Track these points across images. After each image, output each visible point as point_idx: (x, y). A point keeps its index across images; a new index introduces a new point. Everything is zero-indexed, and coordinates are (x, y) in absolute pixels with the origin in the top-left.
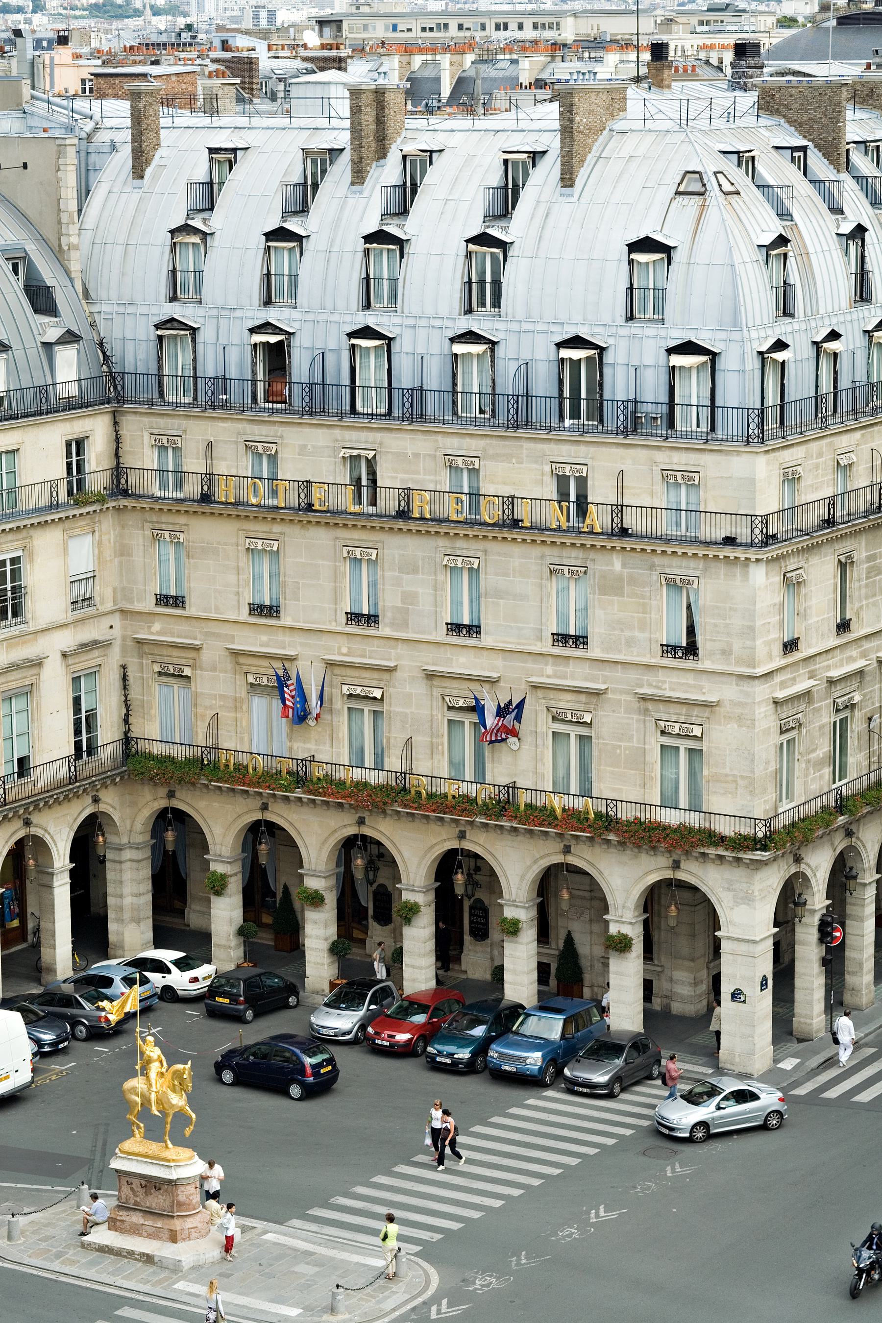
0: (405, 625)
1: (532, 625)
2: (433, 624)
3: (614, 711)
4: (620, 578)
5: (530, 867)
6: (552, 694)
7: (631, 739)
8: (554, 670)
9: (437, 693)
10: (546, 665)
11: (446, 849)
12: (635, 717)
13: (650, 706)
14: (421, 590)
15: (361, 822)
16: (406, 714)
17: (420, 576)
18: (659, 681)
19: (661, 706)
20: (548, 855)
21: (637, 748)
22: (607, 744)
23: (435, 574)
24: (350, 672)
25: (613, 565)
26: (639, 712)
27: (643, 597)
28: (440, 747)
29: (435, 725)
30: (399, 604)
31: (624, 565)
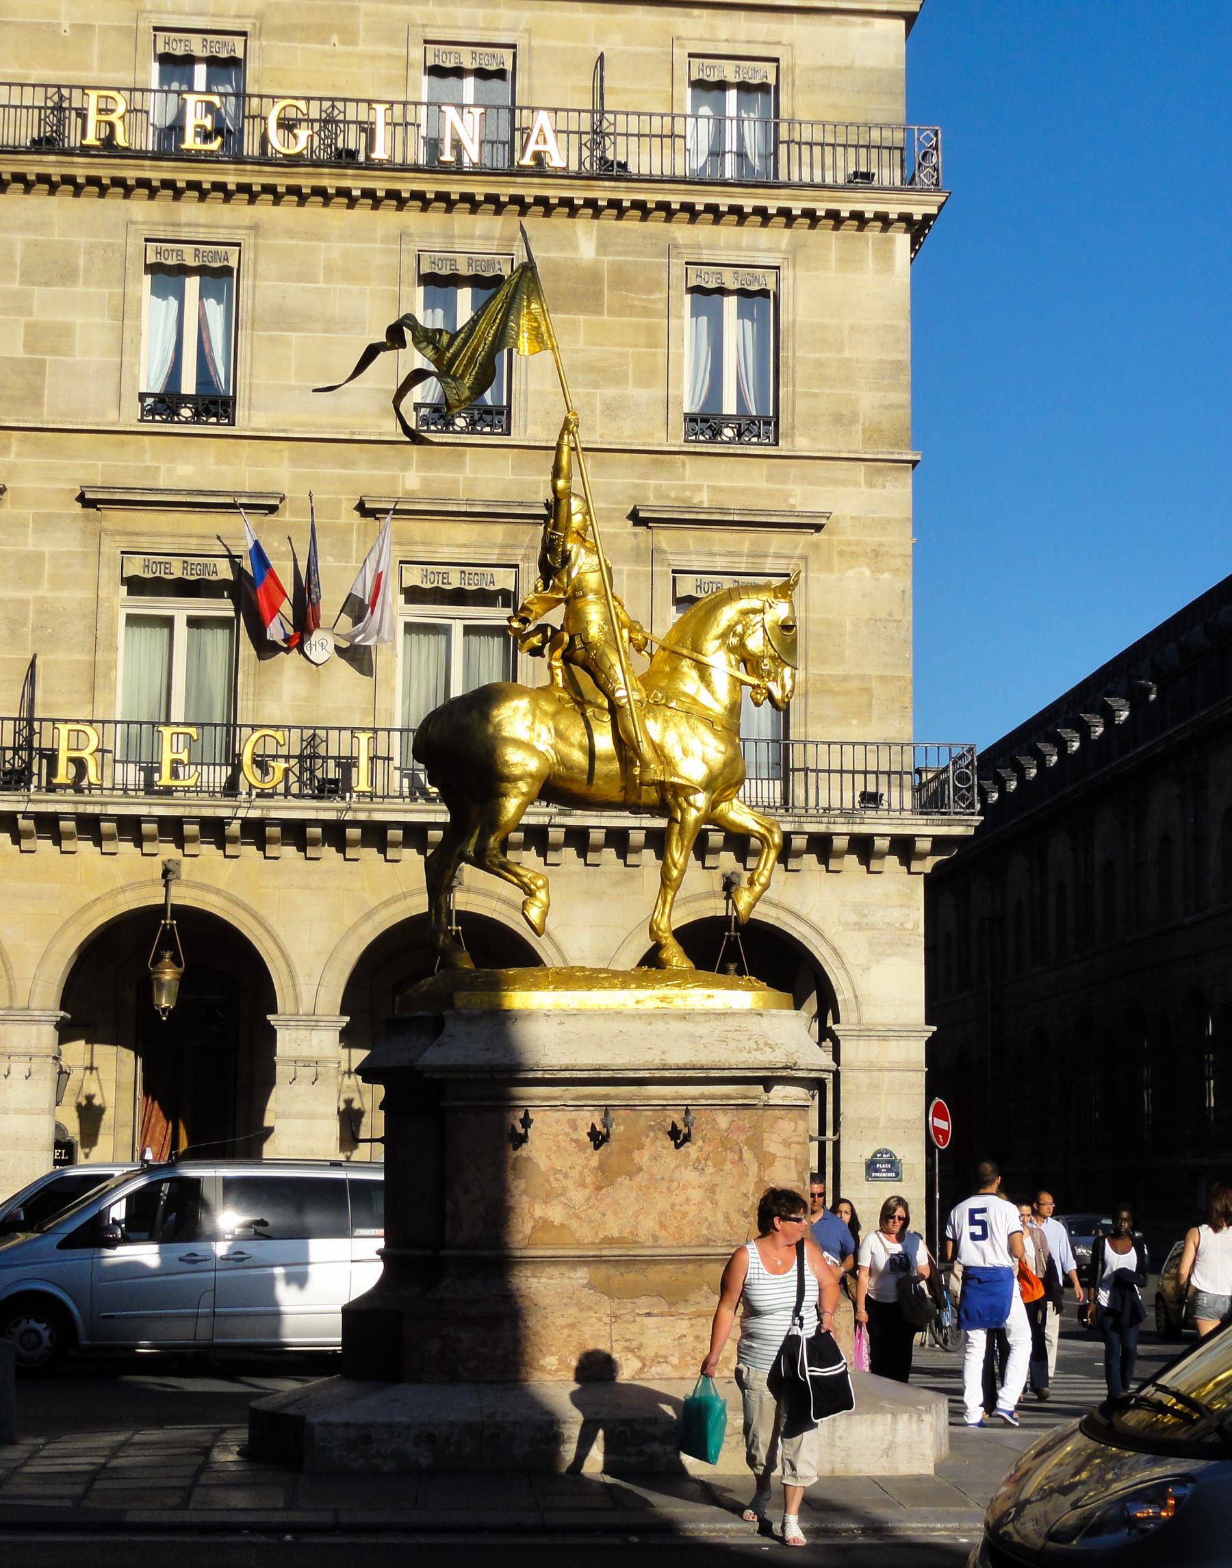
0: (34, 396)
2: (111, 395)
4: (593, 276)
5: (355, 926)
6: (417, 528)
8: (424, 479)
9: (112, 548)
10: (405, 468)
13: (664, 538)
14: (78, 320)
16: (24, 603)
17: (80, 289)
18: (684, 488)
25: (575, 248)
26: (636, 555)
27: (646, 312)
30: (20, 353)
31: (602, 247)
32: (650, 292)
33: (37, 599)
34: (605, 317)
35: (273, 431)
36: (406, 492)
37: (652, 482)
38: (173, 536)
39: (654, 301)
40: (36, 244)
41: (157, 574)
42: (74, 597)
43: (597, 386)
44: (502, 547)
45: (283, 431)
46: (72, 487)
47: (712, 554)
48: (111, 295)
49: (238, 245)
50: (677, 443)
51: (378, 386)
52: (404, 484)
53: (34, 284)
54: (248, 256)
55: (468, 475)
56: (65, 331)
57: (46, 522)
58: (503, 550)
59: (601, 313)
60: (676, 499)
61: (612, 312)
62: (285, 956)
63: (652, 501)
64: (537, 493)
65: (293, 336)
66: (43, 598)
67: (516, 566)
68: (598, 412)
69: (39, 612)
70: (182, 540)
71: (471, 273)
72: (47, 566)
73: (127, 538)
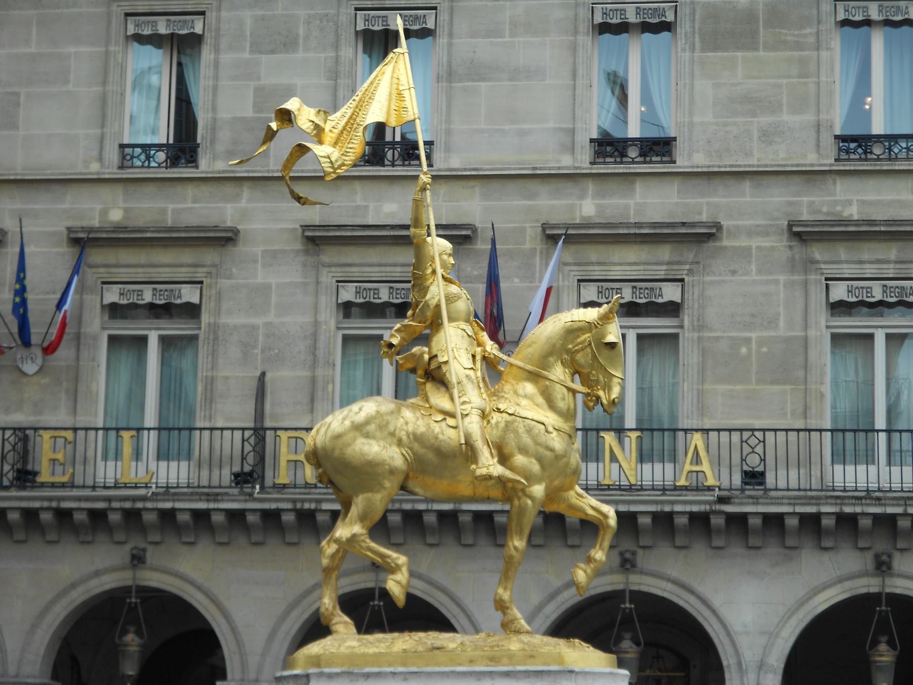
1: (551, 125)
3: (734, 272)
7: (773, 322)
8: (598, 206)
9: (328, 278)
10: (582, 197)
12: (782, 278)
13: (817, 252)
15: (138, 559)
16: (254, 328)
17: (300, 55)
18: (836, 203)
19: (842, 251)
21: (788, 340)
22: (717, 339)
23: (336, 47)
24: (126, 256)
26: (792, 266)
28: (330, 387)
29: (321, 344)
30: (249, 113)
32: (802, 27)
33: (268, 325)
34: (762, 53)
35: (465, 170)
36: (583, 218)
37: (805, 199)
38: (380, 265)
39: (805, 36)
40: (263, 18)
41: (367, 299)
42: (297, 321)
43: (754, 114)
44: (669, 263)
45: (474, 169)
46: (291, 226)
47: (861, 262)
48: (326, 59)
49: (435, 8)
50: (828, 160)
51: (557, 126)
52: (581, 211)
53: (261, 52)
54: (444, 17)
55: (638, 200)
57: (273, 257)
58: (670, 267)
59: (757, 49)
60: (828, 214)
61: (767, 48)
63: (805, 217)
64: (700, 213)
65: (483, 84)
66: (271, 323)
67: (682, 280)
68: (755, 138)
69: (267, 336)
70: (388, 269)
71: (638, 20)
72: (273, 296)
73: (339, 269)
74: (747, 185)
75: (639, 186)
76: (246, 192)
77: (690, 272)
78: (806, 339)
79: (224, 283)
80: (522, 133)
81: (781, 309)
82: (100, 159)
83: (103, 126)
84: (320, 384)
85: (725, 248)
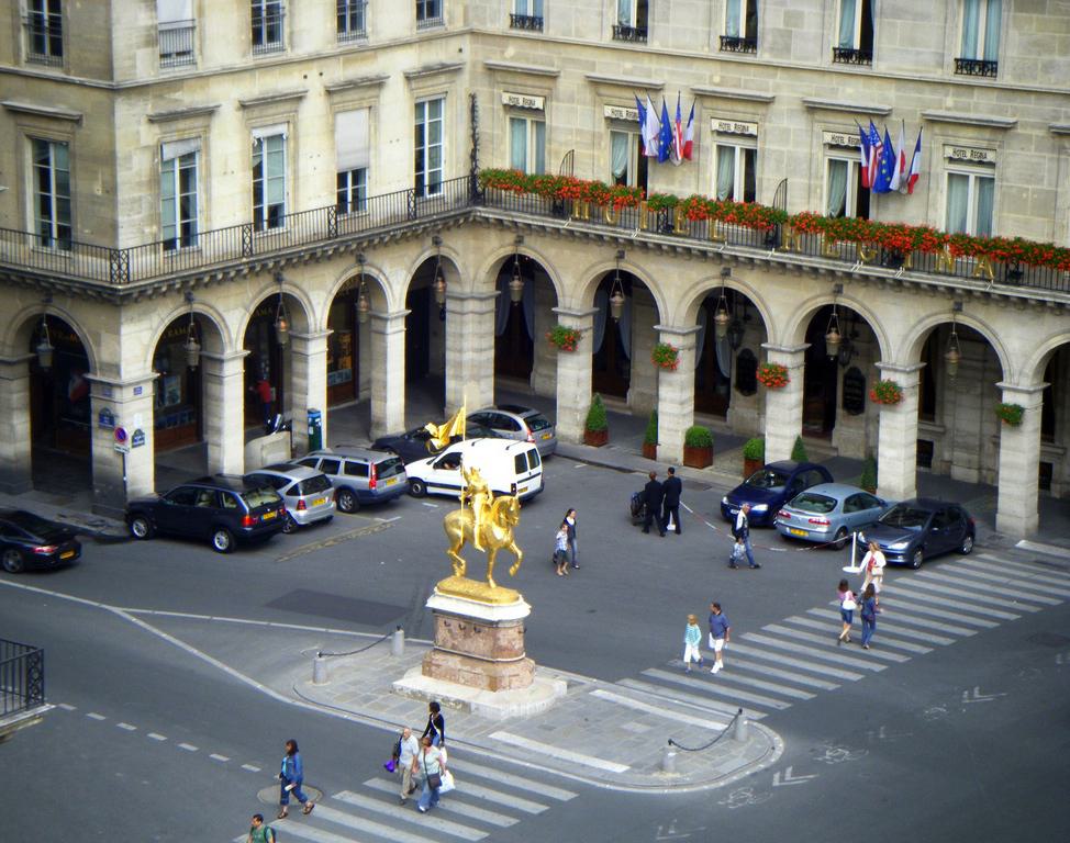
0: (787, 49)
1: (933, 50)
2: (818, 50)
3: (1022, 149)
6: (951, 130)
8: (955, 102)
10: (947, 95)
11: (820, 304)
12: (1048, 155)
16: (782, 152)
20: (936, 314)
21: (1048, 192)
28: (818, 191)
29: (814, 166)
30: (781, 26)
33: (789, 152)
42: (803, 151)
44: (989, 140)
56: (800, 15)
61: (1050, 13)
62: (885, 337)
65: (899, 21)
74: (1033, 97)
75: (976, 92)
76: (779, 73)
77: (1000, 146)
78: (1056, 192)
79: (767, 124)
80: (918, 53)
81: (1046, 174)
82: (709, 45)
83: (710, 26)
84: (813, 188)
85: (1019, 134)
